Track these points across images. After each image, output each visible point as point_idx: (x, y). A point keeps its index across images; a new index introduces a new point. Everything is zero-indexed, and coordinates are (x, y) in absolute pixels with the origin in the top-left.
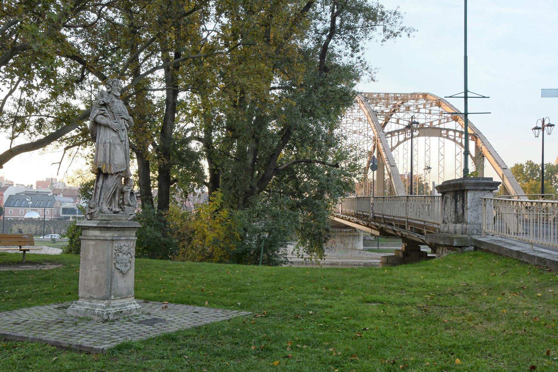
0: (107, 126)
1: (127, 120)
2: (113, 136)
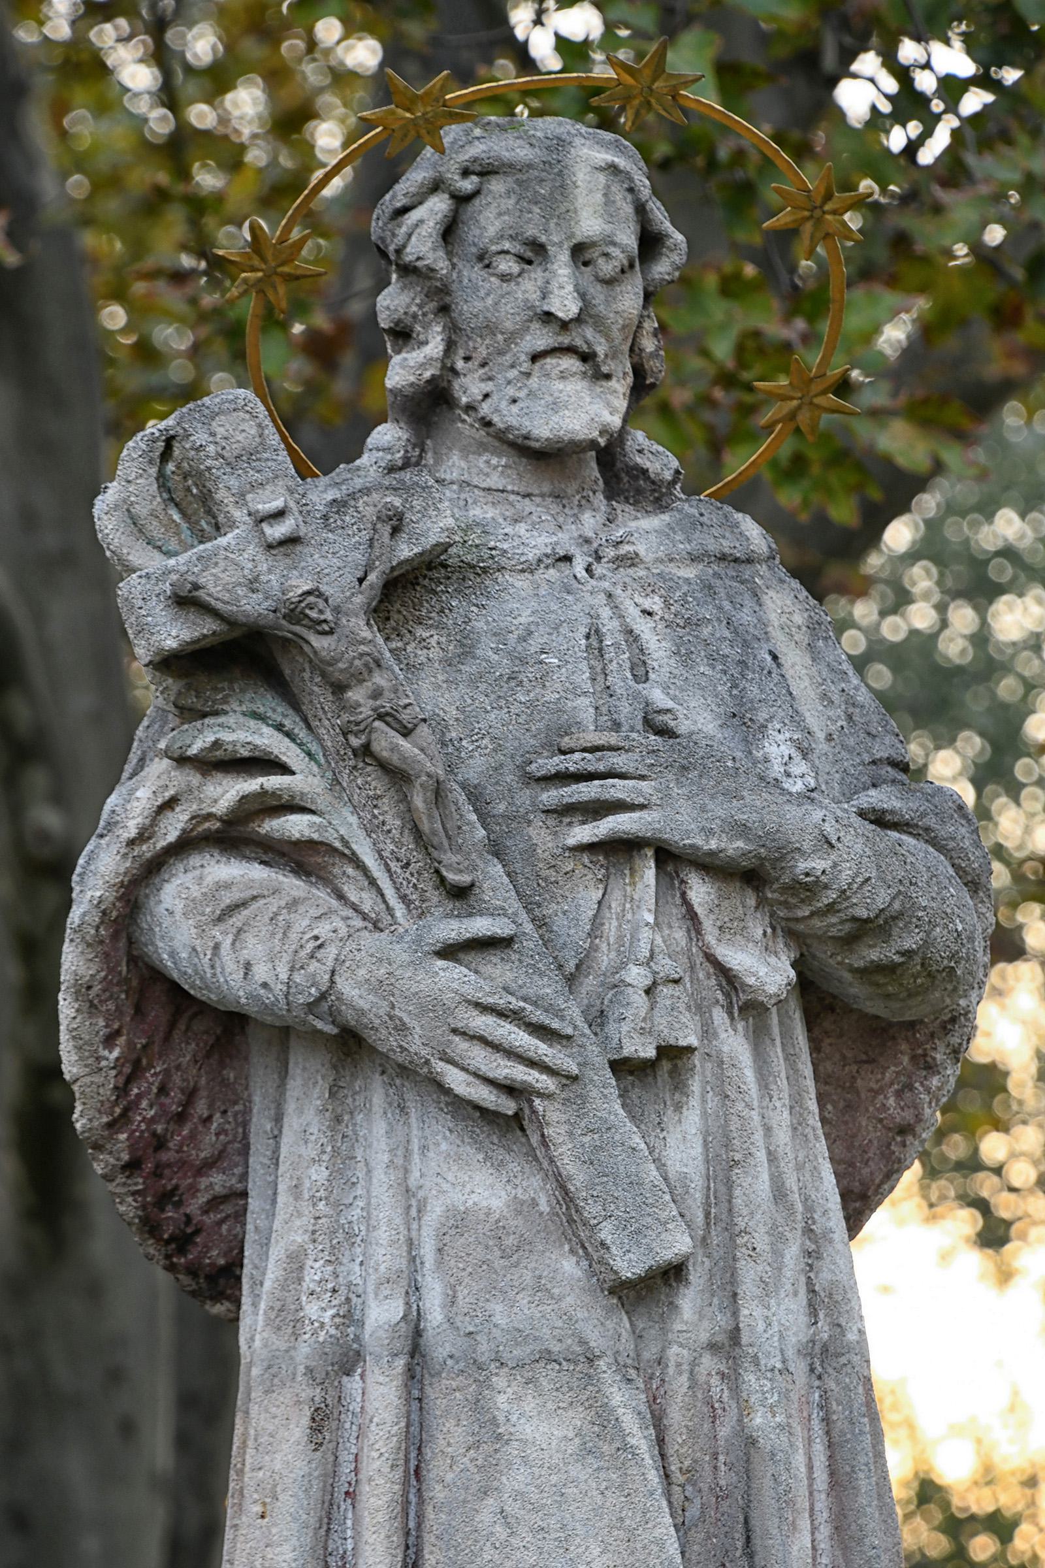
2: (458, 1221)
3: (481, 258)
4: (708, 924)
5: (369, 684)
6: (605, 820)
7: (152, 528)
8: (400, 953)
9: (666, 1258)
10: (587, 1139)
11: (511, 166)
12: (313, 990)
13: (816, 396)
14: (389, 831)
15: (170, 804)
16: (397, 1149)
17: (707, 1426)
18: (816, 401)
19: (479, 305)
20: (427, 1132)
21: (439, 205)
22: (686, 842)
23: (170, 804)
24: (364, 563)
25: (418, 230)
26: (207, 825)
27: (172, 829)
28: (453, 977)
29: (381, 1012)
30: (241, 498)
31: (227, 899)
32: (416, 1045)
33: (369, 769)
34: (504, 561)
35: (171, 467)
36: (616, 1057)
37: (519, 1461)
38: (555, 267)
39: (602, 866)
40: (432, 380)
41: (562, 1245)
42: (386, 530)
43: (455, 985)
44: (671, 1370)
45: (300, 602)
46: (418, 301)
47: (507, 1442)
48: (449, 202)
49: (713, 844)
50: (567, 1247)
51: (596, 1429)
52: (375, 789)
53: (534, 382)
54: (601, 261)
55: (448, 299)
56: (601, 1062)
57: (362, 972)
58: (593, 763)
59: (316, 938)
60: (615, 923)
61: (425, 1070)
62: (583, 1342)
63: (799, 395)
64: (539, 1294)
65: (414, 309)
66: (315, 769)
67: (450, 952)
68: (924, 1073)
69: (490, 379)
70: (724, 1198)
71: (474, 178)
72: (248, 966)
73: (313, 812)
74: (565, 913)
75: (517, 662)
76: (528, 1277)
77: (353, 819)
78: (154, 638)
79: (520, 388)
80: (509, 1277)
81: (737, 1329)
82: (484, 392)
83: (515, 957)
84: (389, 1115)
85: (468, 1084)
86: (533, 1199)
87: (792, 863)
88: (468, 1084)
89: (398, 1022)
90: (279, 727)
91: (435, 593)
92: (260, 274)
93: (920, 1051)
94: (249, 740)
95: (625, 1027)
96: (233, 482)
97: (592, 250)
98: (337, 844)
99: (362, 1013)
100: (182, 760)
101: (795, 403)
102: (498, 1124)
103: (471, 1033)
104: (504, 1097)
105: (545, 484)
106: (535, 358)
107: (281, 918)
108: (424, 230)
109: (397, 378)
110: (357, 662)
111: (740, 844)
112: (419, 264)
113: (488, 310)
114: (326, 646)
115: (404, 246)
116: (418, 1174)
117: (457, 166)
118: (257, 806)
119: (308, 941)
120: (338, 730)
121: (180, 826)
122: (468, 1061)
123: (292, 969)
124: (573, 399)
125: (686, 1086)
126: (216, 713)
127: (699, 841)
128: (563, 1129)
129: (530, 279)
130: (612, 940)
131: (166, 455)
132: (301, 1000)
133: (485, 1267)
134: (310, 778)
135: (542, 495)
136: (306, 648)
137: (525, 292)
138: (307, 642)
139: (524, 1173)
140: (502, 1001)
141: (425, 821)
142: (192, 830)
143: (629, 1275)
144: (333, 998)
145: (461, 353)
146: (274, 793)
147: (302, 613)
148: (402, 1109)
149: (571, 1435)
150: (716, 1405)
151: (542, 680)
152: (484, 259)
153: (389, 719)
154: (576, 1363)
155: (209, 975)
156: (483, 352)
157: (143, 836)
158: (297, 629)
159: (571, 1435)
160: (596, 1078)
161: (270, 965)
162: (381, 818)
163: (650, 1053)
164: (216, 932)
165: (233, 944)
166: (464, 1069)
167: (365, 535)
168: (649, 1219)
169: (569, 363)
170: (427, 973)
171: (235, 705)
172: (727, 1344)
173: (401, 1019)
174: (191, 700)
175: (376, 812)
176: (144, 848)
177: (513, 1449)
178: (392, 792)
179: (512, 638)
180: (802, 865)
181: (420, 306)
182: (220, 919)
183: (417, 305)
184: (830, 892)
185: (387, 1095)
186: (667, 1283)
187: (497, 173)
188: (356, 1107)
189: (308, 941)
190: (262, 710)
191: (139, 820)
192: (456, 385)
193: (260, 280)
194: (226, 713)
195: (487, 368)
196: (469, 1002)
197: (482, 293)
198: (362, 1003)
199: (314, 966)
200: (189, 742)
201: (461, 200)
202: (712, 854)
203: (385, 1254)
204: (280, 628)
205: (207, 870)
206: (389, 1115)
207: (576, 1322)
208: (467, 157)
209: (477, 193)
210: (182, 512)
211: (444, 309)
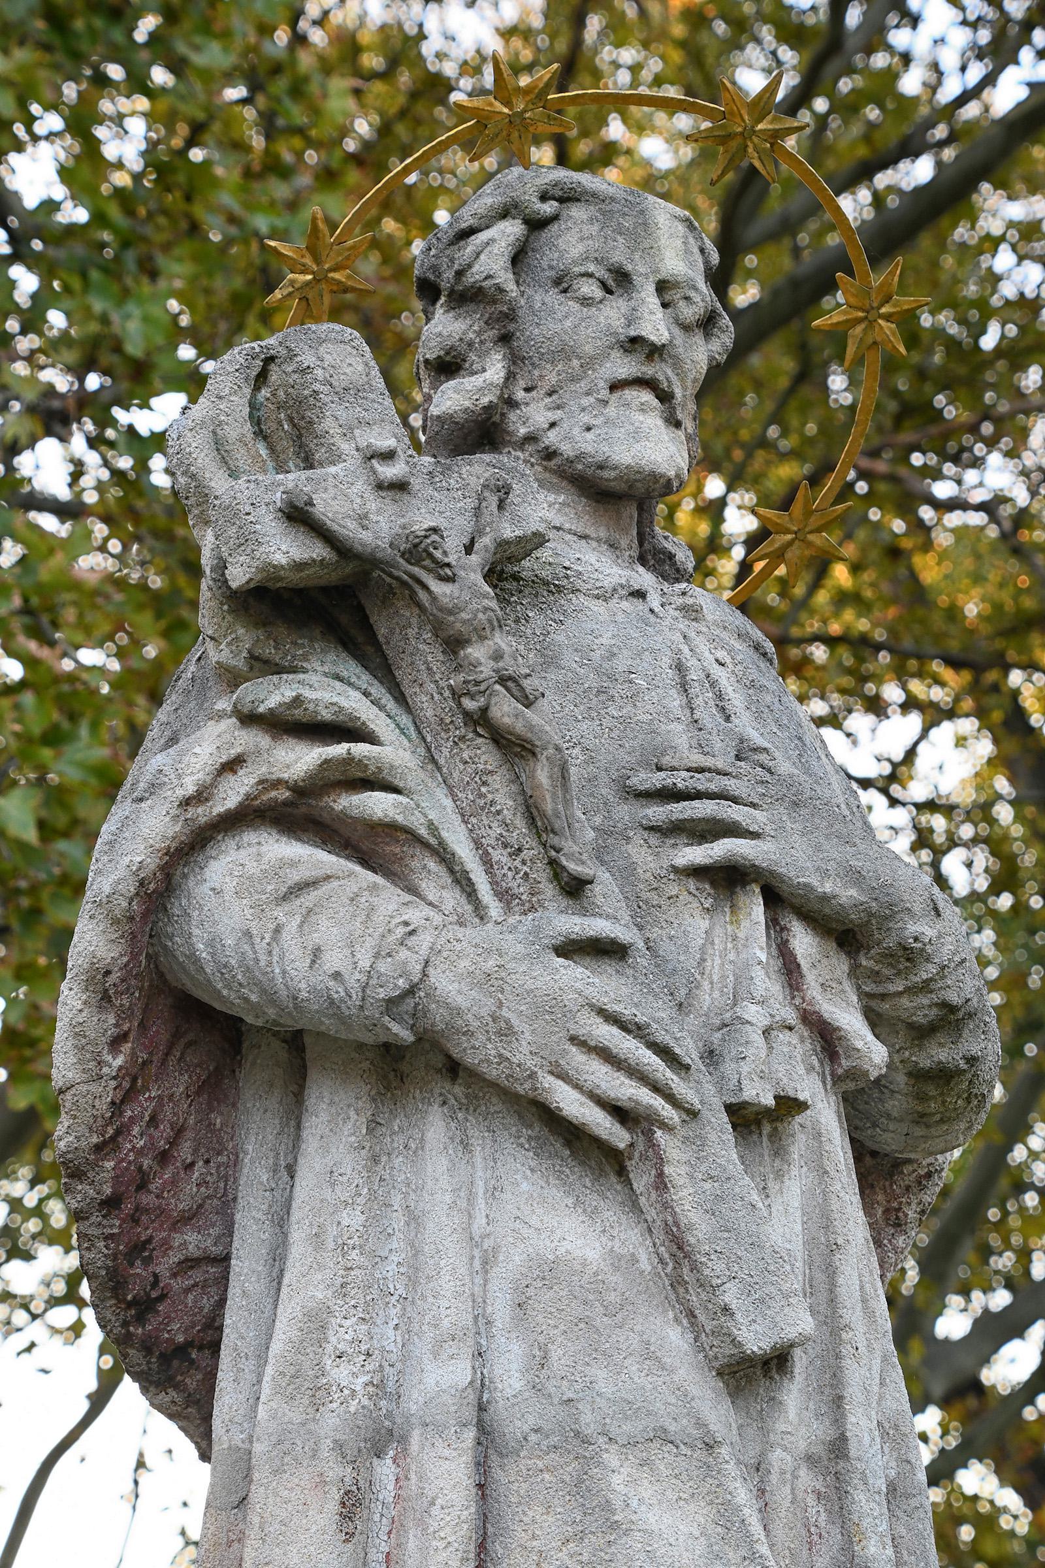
0: (408, 1060)
1: (846, 934)
2: (549, 1271)
3: (557, 282)
4: (811, 979)
5: (491, 643)
6: (722, 841)
7: (238, 456)
8: (514, 945)
9: (790, 1336)
10: (707, 1186)
11: (594, 195)
12: (401, 982)
13: (811, 532)
14: (498, 812)
15: (232, 766)
16: (459, 1190)
17: (805, 1552)
18: (811, 537)
19: (558, 327)
20: (501, 1171)
21: (510, 230)
22: (801, 880)
23: (232, 766)
24: (470, 530)
25: (489, 248)
26: (273, 794)
27: (232, 794)
28: (575, 977)
29: (484, 1012)
30: (348, 433)
31: (295, 876)
32: (522, 1053)
33: (480, 740)
34: (579, 584)
35: (265, 393)
36: (733, 1100)
37: (643, 1556)
38: (643, 295)
39: (709, 894)
40: (489, 408)
41: (665, 1311)
42: (493, 500)
43: (578, 985)
44: (774, 1478)
45: (426, 537)
46: (476, 328)
47: (626, 1533)
48: (523, 227)
49: (828, 887)
50: (671, 1315)
51: (719, 1529)
52: (486, 763)
53: (611, 411)
54: (682, 304)
55: (511, 327)
56: (717, 1103)
57: (464, 964)
58: (702, 783)
59: (406, 924)
60: (718, 961)
61: (527, 1085)
62: (700, 1424)
63: (795, 529)
64: (647, 1362)
65: (472, 336)
66: (406, 742)
67: (571, 949)
68: (892, 1231)
69: (558, 407)
70: (823, 1287)
71: (555, 204)
72: (317, 953)
73: (396, 790)
74: (671, 938)
75: (605, 678)
76: (635, 1341)
77: (448, 802)
78: (261, 549)
79: (595, 416)
80: (614, 1338)
81: (843, 1438)
82: (551, 420)
83: (630, 972)
84: (450, 1152)
85: (582, 1104)
86: (633, 1255)
87: (900, 925)
88: (582, 1104)
89: (503, 1025)
90: (366, 694)
91: (509, 602)
92: (310, 277)
93: (895, 1205)
94: (335, 700)
95: (745, 1068)
96: (341, 413)
97: (674, 292)
98: (423, 832)
99: (459, 1012)
100: (249, 719)
101: (789, 537)
102: (590, 1167)
103: (593, 1043)
104: (619, 1126)
105: (602, 528)
106: (615, 387)
107: (363, 900)
108: (496, 249)
109: (449, 403)
110: (480, 615)
111: (852, 892)
112: (486, 284)
113: (566, 333)
114: (448, 592)
115: (470, 266)
116: (484, 1221)
117: (534, 188)
118: (338, 776)
119: (397, 926)
120: (447, 693)
121: (243, 790)
122: (585, 1077)
123: (377, 956)
124: (654, 432)
125: (787, 1153)
126: (293, 670)
127: (814, 881)
128: (683, 1170)
129: (612, 307)
130: (715, 978)
131: (262, 378)
132: (382, 994)
133: (582, 1325)
134: (401, 751)
135: (599, 540)
136: (422, 595)
137: (607, 318)
138: (425, 587)
139: (621, 1225)
140: (626, 1012)
141: (549, 800)
142: (256, 798)
143: (755, 1349)
144: (422, 994)
145: (522, 383)
146: (360, 761)
147: (425, 550)
148: (466, 1146)
149: (697, 1533)
150: (813, 1529)
151: (633, 698)
152: (562, 282)
153: (510, 684)
154: (692, 1447)
155: (262, 963)
156: (552, 378)
157: (201, 796)
158: (416, 570)
159: (697, 1533)
160: (713, 1120)
161: (347, 952)
162: (490, 796)
163: (769, 1101)
164: (279, 913)
165: (301, 926)
166: (577, 1087)
167: (471, 503)
168: (772, 1289)
169: (647, 397)
170: (545, 968)
171: (316, 665)
172: (825, 1458)
173: (508, 1021)
174: (268, 651)
175: (483, 789)
176: (200, 810)
177: (635, 1542)
178: (503, 770)
179: (596, 656)
180: (913, 928)
181: (479, 333)
182: (285, 898)
183: (475, 331)
184: (930, 966)
185: (449, 1129)
186: (766, 1373)
187: (578, 200)
188: (393, 1149)
189: (397, 926)
190: (345, 674)
191: (200, 775)
192: (513, 416)
193: (307, 284)
194: (305, 671)
195: (555, 397)
196: (592, 1006)
197: (559, 315)
198: (461, 1001)
199: (404, 954)
200: (262, 697)
201: (536, 225)
202: (825, 898)
203: (447, 1305)
204: (395, 566)
205: (264, 849)
206: (450, 1152)
207: (693, 1399)
208: (547, 181)
209: (555, 218)
210: (272, 449)
211: (505, 339)
